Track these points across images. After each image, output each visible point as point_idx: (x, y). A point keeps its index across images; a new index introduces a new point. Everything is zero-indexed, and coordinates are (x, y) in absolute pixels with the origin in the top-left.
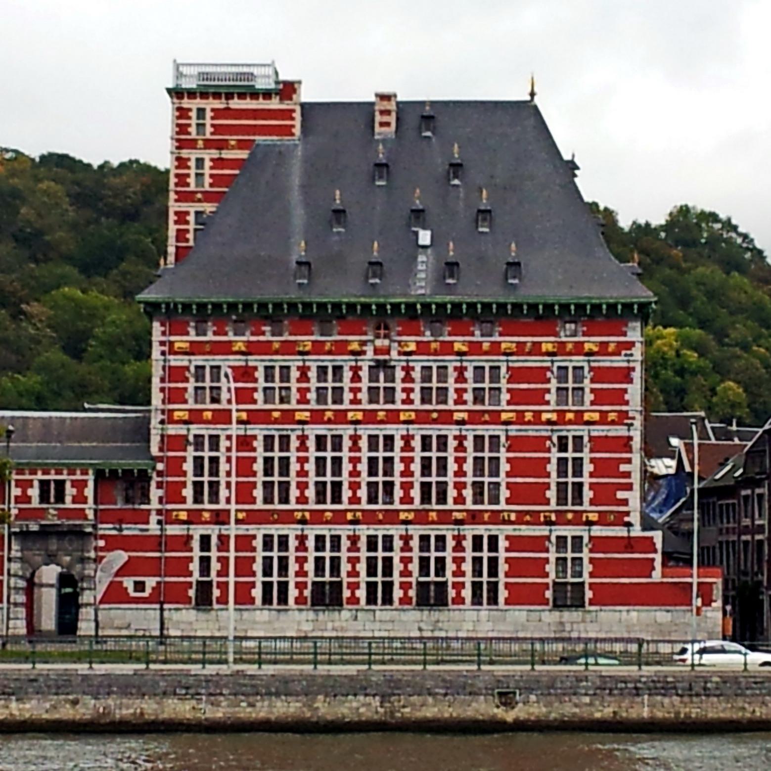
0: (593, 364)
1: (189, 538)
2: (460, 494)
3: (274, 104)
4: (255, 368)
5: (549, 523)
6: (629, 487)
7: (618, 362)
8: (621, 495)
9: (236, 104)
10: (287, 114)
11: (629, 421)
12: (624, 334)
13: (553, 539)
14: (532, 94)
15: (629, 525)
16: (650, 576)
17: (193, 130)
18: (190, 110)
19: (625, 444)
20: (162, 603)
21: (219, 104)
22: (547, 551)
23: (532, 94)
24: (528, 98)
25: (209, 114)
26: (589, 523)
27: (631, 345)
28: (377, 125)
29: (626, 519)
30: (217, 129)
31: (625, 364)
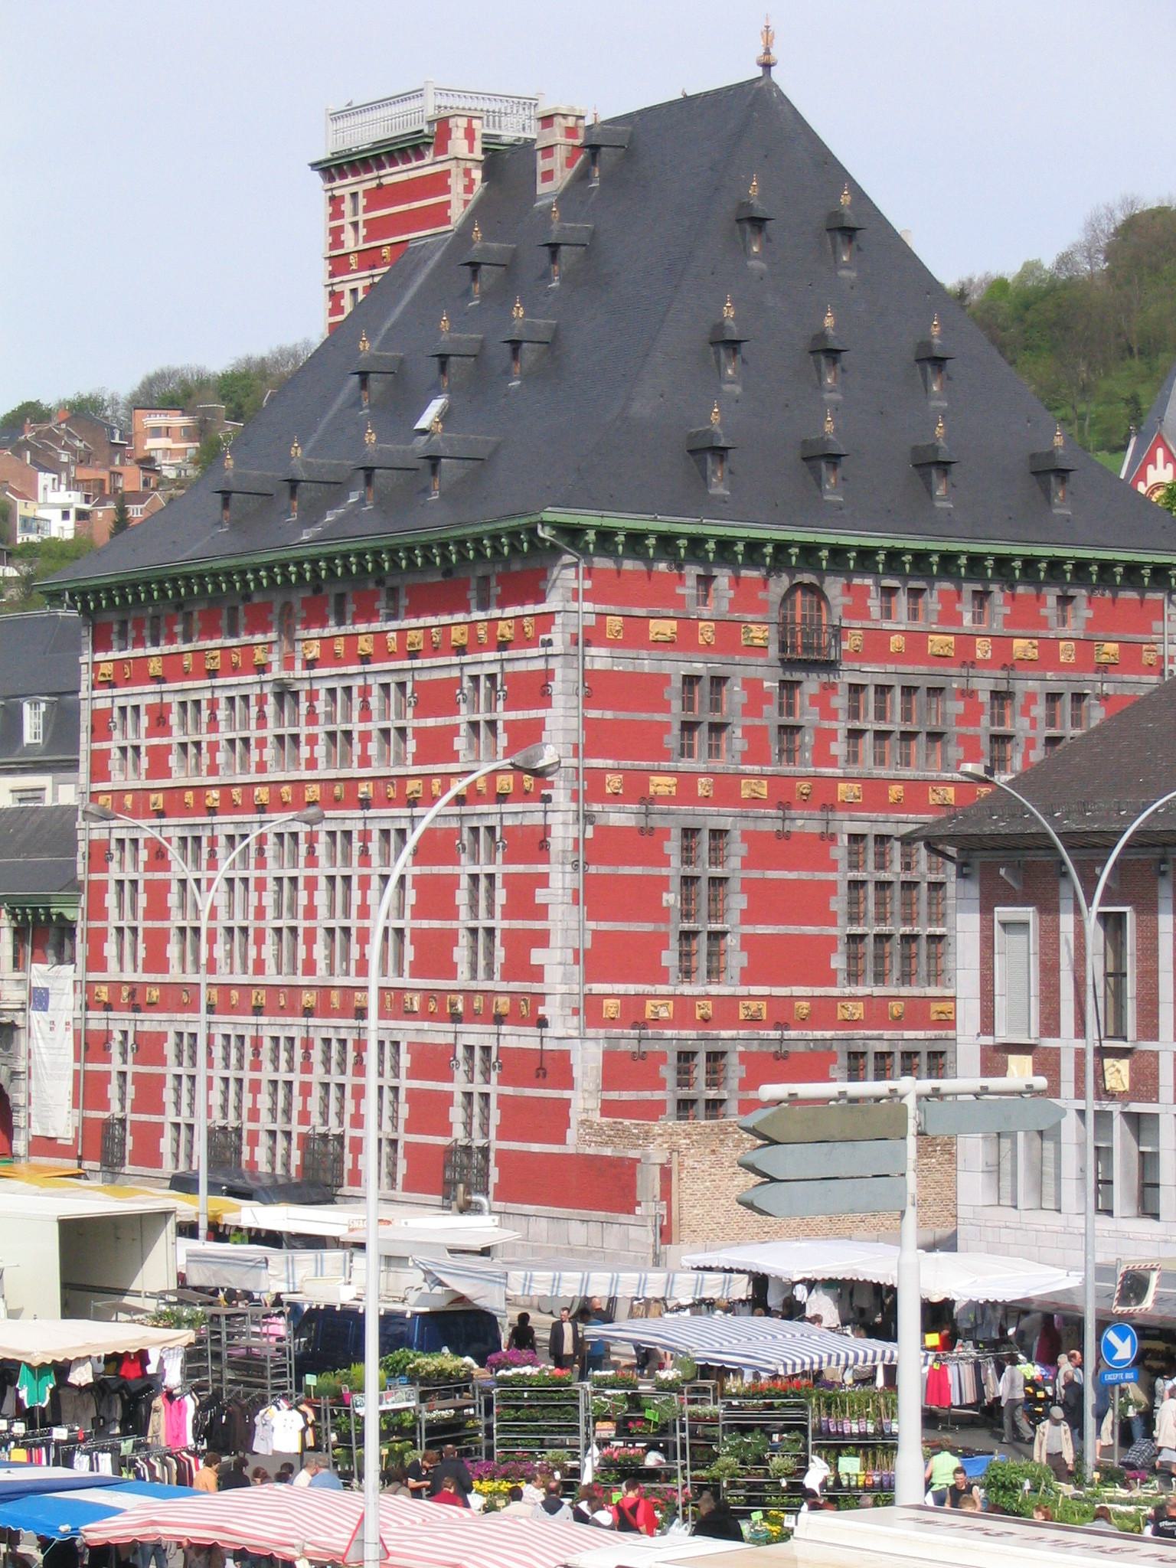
0: (509, 668)
1: (109, 1033)
2: (363, 955)
3: (425, 167)
4: (169, 705)
5: (456, 1018)
6: (542, 939)
7: (527, 661)
8: (537, 956)
9: (395, 175)
10: (438, 183)
11: (545, 792)
12: (540, 597)
13: (460, 1053)
14: (767, 66)
15: (542, 1023)
16: (562, 1141)
17: (348, 236)
18: (342, 198)
19: (537, 844)
20: (80, 1158)
21: (367, 182)
22: (450, 1078)
23: (767, 66)
24: (759, 72)
25: (362, 202)
26: (499, 1019)
27: (546, 620)
28: (539, 178)
29: (541, 1011)
30: (376, 229)
31: (539, 665)
